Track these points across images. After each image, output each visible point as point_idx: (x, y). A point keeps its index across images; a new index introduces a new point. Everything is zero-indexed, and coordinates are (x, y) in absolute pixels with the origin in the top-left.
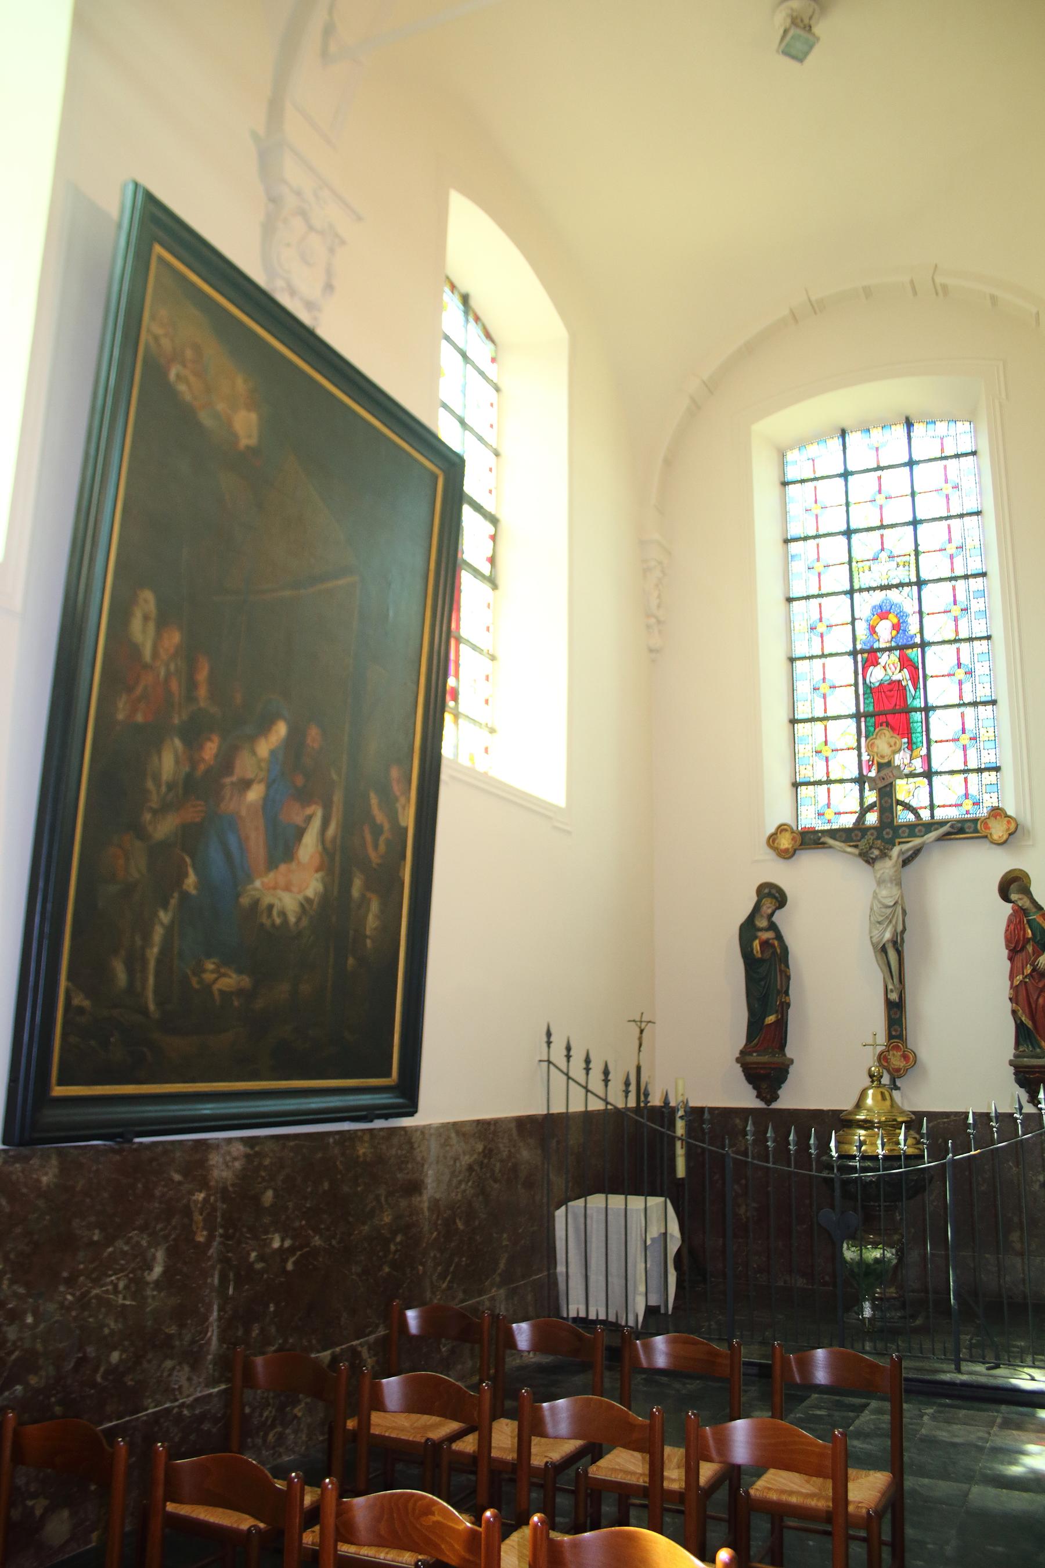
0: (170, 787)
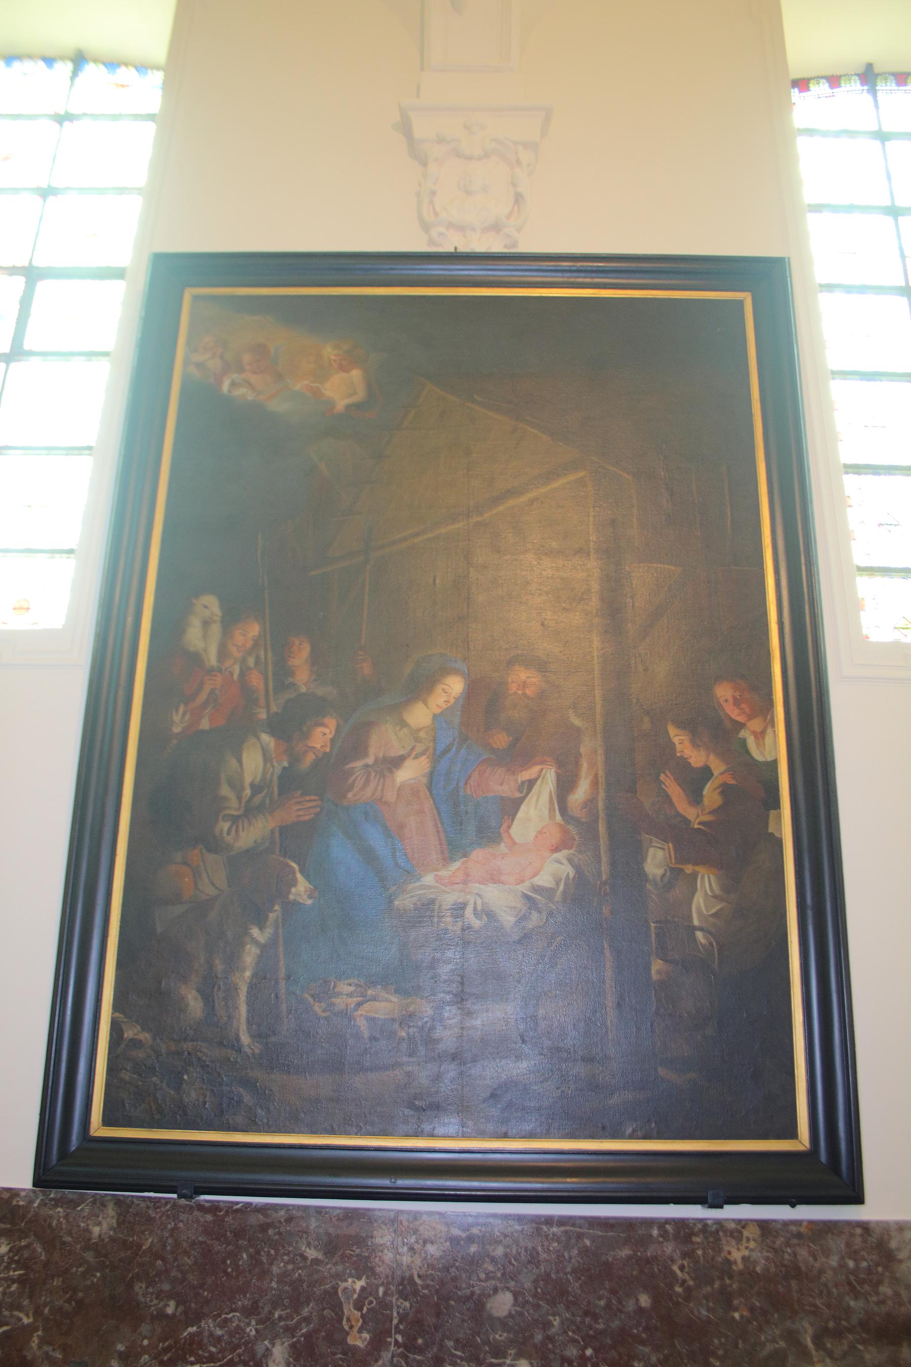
0: (256, 788)
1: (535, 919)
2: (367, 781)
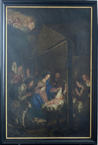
1: (59, 109)
2: (38, 90)
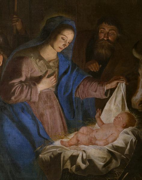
1: (114, 164)
2: (22, 91)
